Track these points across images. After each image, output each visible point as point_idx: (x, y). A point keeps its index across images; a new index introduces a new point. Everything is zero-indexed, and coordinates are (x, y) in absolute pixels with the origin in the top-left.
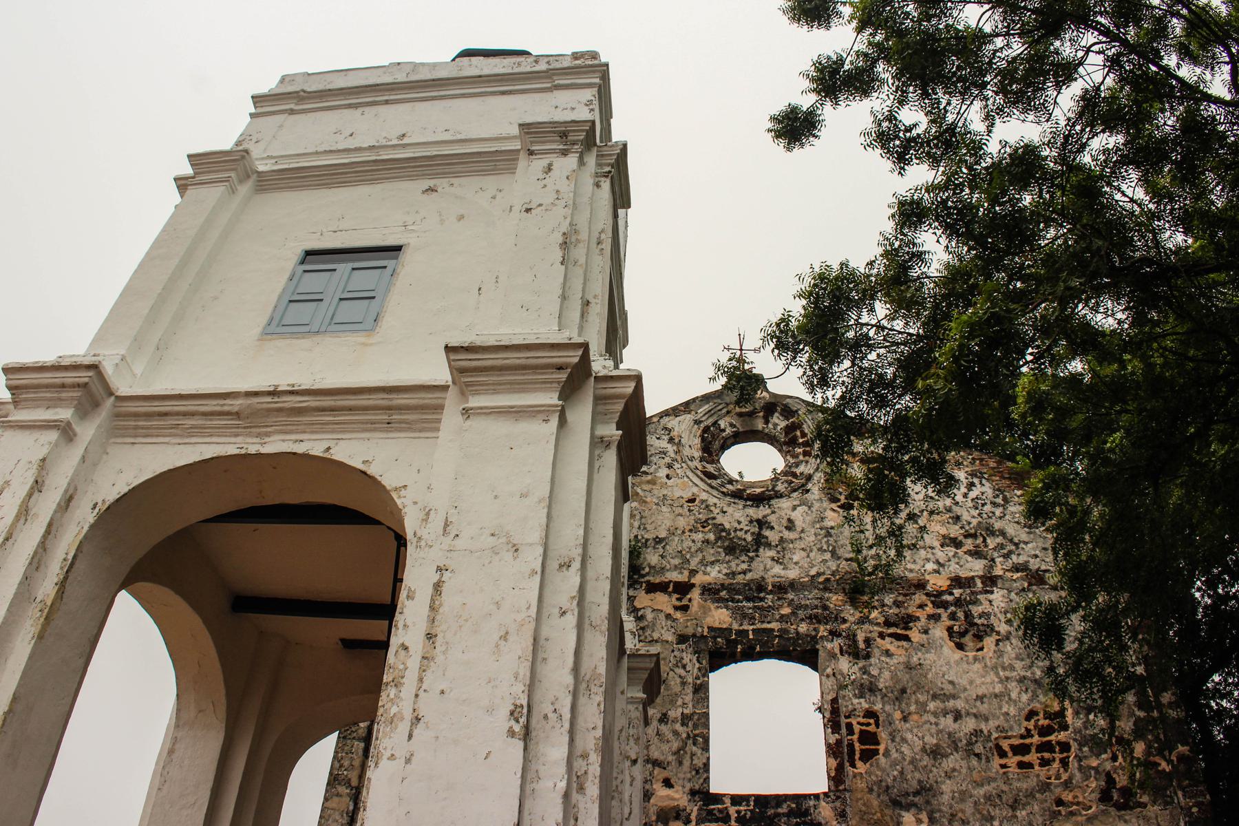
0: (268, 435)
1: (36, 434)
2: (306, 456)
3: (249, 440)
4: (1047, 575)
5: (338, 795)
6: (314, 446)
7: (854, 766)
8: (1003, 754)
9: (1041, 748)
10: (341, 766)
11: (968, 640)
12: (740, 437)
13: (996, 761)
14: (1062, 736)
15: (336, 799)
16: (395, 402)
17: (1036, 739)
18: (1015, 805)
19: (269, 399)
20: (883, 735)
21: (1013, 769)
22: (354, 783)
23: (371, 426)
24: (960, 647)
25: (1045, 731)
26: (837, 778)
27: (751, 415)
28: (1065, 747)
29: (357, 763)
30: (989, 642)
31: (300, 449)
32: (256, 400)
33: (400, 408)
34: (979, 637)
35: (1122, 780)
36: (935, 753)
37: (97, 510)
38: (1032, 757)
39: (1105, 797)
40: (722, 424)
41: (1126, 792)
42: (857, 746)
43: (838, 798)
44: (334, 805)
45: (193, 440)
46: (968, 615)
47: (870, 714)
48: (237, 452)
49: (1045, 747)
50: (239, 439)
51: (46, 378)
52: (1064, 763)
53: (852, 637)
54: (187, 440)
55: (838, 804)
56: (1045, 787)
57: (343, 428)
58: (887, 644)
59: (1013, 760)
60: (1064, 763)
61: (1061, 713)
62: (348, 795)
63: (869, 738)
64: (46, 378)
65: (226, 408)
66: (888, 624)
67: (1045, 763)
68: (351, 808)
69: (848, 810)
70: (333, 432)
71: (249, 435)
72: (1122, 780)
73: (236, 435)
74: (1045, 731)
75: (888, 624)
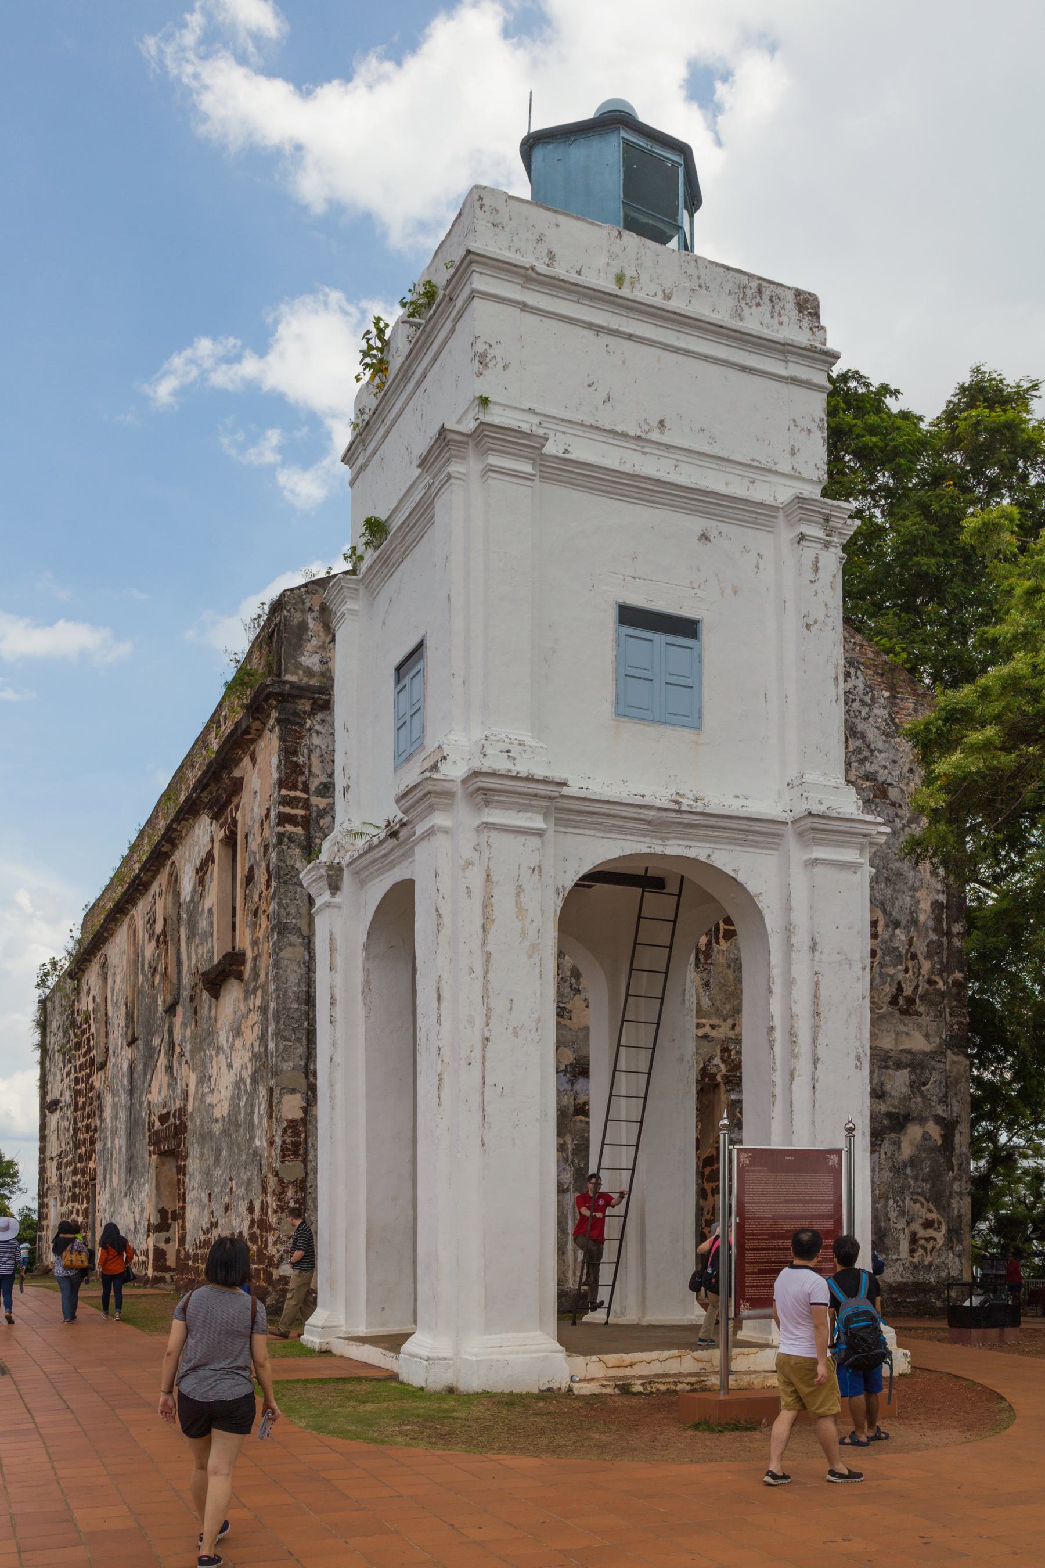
0: (667, 839)
1: (522, 839)
2: (695, 860)
3: (654, 841)
4: (890, 788)
5: (291, 944)
6: (699, 851)
7: (718, 943)
10: (288, 914)
15: (289, 949)
16: (753, 828)
19: (673, 815)
22: (305, 932)
23: (733, 842)
29: (304, 911)
31: (691, 853)
32: (665, 814)
33: (755, 832)
37: (561, 895)
42: (722, 924)
43: (706, 969)
44: (289, 955)
45: (613, 835)
48: (648, 850)
50: (647, 839)
51: (519, 787)
54: (609, 835)
55: (705, 975)
57: (718, 840)
62: (302, 944)
64: (519, 787)
65: (642, 816)
68: (307, 958)
69: (711, 980)
70: (710, 842)
71: (655, 837)
73: (645, 836)
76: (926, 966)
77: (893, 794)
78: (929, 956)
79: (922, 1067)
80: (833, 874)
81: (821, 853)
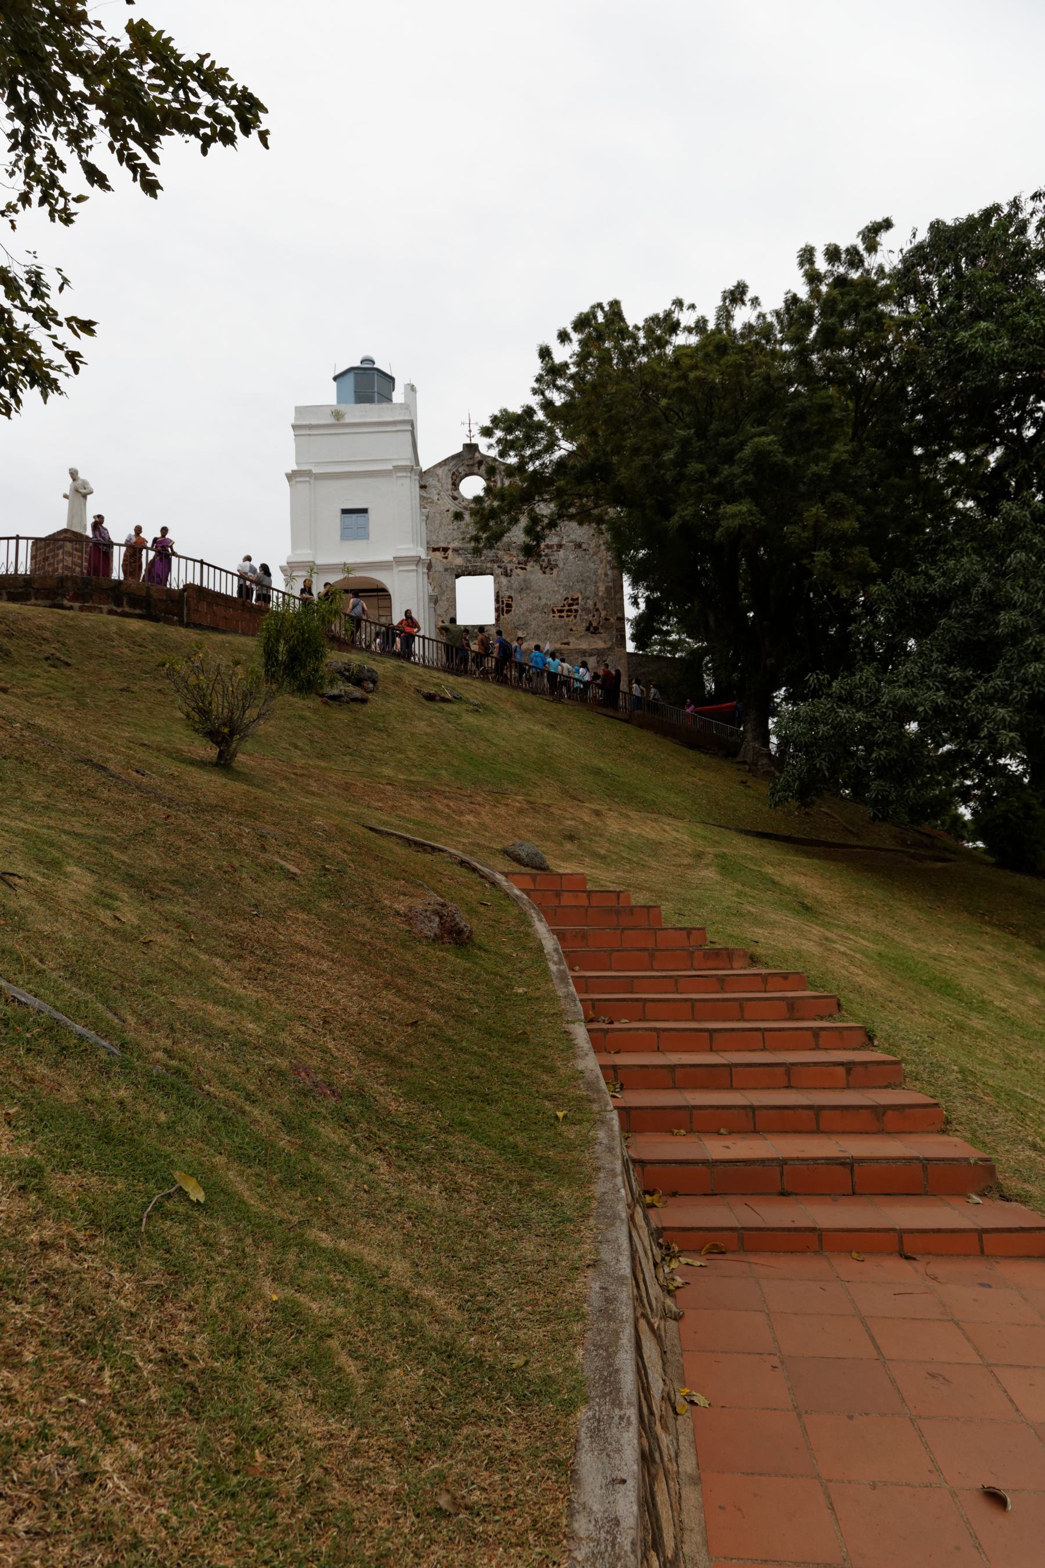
8: (554, 612)
9: (568, 611)
11: (548, 570)
12: (467, 475)
13: (552, 615)
14: (575, 607)
17: (567, 608)
18: (556, 629)
20: (514, 604)
21: (557, 618)
24: (544, 573)
25: (570, 605)
26: (497, 619)
27: (472, 465)
28: (576, 611)
30: (555, 571)
34: (552, 569)
35: (595, 624)
36: (531, 611)
38: (564, 614)
39: (588, 629)
40: (460, 470)
41: (596, 628)
46: (549, 560)
47: (510, 597)
49: (570, 611)
52: (575, 617)
53: (506, 569)
56: (567, 624)
58: (519, 571)
59: (557, 615)
60: (575, 617)
61: (577, 599)
63: (509, 606)
66: (519, 563)
67: (568, 616)
72: (595, 624)
74: (570, 605)
75: (519, 563)
76: (603, 613)
77: (584, 546)
78: (605, 609)
79: (603, 655)
80: (406, 574)
81: (401, 568)
